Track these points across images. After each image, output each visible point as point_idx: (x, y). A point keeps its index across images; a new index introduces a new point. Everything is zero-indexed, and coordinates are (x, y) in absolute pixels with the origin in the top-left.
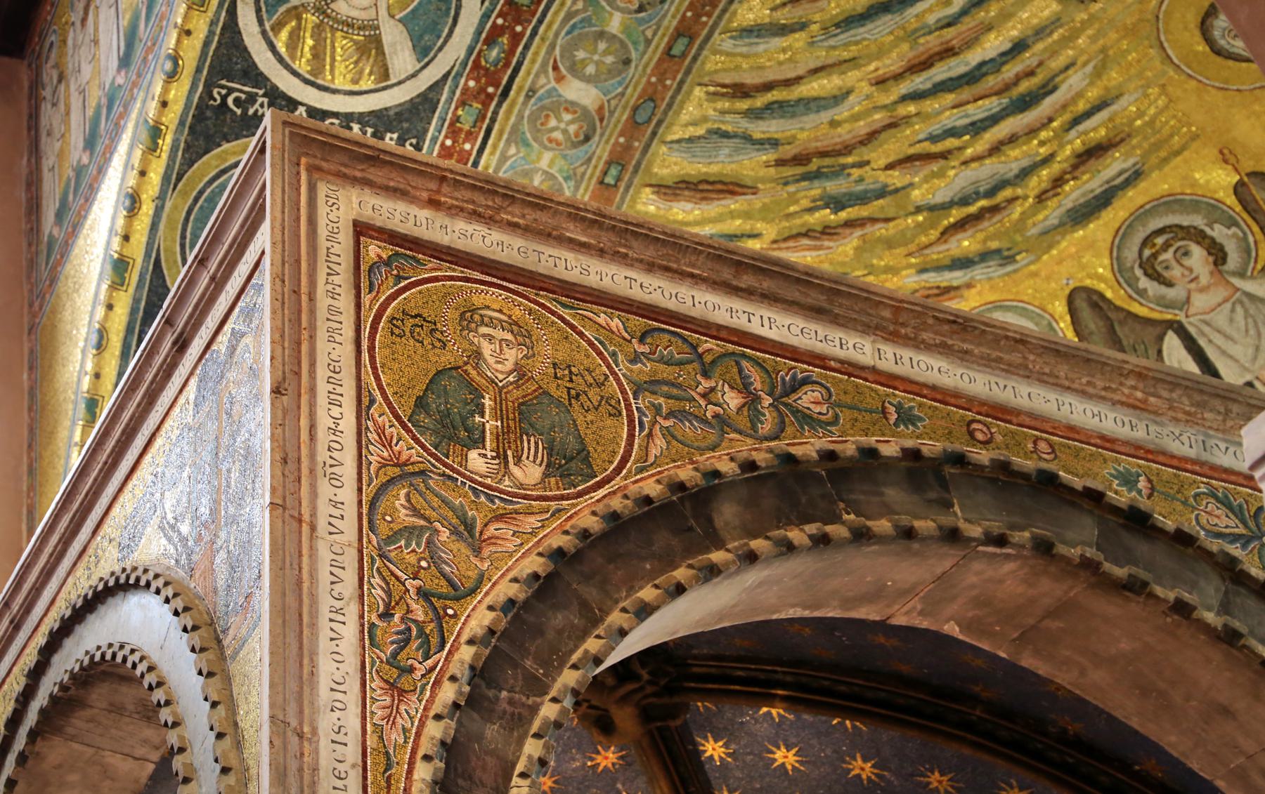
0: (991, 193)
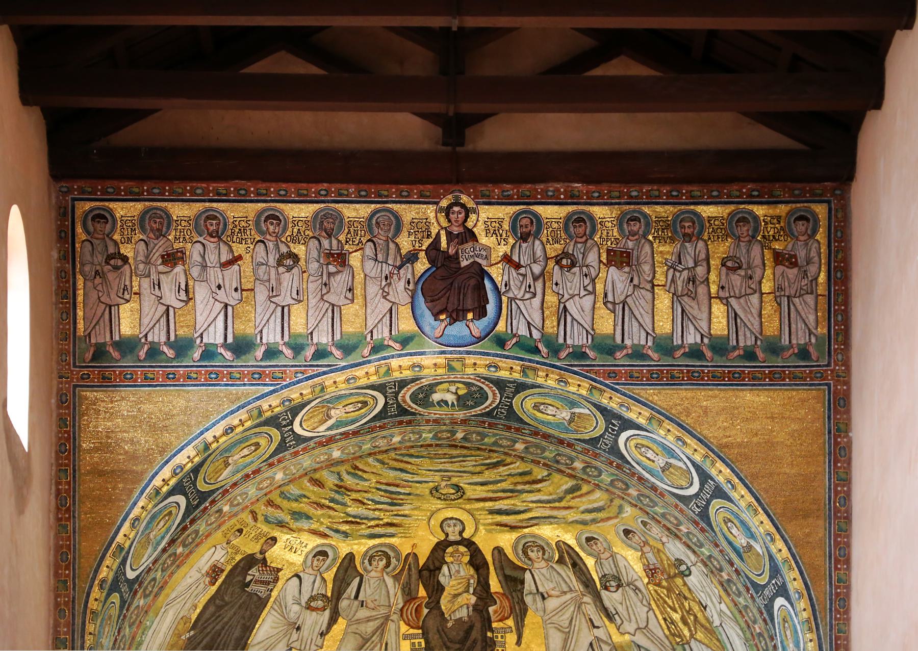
0: (362, 519)
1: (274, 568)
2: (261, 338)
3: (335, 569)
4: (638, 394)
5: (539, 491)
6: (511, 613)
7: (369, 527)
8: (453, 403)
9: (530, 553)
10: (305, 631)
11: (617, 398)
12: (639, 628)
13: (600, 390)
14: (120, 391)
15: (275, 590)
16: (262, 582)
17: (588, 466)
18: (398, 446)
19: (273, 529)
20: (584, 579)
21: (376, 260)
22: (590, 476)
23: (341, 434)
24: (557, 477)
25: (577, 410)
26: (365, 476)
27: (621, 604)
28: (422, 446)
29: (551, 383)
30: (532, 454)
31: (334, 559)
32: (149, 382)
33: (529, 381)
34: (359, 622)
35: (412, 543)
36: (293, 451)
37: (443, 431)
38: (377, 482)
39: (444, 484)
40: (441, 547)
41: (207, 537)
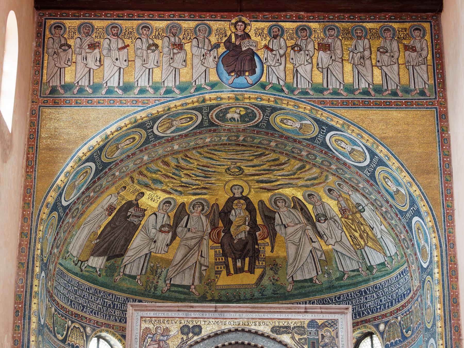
0: (189, 185)
1: (142, 209)
2: (138, 84)
3: (175, 211)
4: (336, 112)
5: (283, 169)
6: (268, 235)
7: (193, 189)
8: (238, 119)
9: (278, 203)
10: (159, 243)
11: (325, 114)
12: (337, 242)
13: (316, 110)
14: (63, 109)
15: (143, 220)
16: (136, 216)
17: (310, 153)
18: (208, 144)
19: (142, 188)
20: (307, 217)
21: (198, 47)
22: (310, 159)
23: (179, 136)
24: (293, 161)
25: (304, 122)
26: (191, 161)
27: (327, 229)
28: (221, 144)
29: (290, 107)
30: (279, 148)
31: (175, 206)
32: (78, 104)
33: (278, 106)
34: (187, 239)
35: (216, 198)
36: (153, 143)
37: (233, 136)
38: (198, 165)
39: (233, 166)
40: (231, 201)
41: (107, 188)
